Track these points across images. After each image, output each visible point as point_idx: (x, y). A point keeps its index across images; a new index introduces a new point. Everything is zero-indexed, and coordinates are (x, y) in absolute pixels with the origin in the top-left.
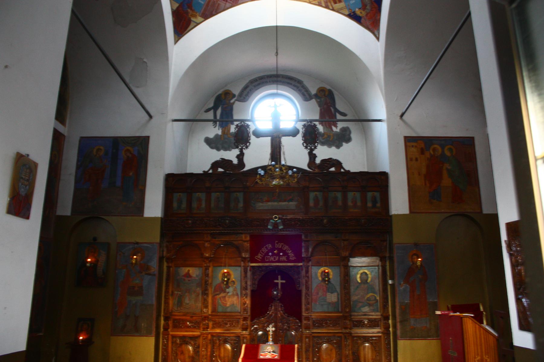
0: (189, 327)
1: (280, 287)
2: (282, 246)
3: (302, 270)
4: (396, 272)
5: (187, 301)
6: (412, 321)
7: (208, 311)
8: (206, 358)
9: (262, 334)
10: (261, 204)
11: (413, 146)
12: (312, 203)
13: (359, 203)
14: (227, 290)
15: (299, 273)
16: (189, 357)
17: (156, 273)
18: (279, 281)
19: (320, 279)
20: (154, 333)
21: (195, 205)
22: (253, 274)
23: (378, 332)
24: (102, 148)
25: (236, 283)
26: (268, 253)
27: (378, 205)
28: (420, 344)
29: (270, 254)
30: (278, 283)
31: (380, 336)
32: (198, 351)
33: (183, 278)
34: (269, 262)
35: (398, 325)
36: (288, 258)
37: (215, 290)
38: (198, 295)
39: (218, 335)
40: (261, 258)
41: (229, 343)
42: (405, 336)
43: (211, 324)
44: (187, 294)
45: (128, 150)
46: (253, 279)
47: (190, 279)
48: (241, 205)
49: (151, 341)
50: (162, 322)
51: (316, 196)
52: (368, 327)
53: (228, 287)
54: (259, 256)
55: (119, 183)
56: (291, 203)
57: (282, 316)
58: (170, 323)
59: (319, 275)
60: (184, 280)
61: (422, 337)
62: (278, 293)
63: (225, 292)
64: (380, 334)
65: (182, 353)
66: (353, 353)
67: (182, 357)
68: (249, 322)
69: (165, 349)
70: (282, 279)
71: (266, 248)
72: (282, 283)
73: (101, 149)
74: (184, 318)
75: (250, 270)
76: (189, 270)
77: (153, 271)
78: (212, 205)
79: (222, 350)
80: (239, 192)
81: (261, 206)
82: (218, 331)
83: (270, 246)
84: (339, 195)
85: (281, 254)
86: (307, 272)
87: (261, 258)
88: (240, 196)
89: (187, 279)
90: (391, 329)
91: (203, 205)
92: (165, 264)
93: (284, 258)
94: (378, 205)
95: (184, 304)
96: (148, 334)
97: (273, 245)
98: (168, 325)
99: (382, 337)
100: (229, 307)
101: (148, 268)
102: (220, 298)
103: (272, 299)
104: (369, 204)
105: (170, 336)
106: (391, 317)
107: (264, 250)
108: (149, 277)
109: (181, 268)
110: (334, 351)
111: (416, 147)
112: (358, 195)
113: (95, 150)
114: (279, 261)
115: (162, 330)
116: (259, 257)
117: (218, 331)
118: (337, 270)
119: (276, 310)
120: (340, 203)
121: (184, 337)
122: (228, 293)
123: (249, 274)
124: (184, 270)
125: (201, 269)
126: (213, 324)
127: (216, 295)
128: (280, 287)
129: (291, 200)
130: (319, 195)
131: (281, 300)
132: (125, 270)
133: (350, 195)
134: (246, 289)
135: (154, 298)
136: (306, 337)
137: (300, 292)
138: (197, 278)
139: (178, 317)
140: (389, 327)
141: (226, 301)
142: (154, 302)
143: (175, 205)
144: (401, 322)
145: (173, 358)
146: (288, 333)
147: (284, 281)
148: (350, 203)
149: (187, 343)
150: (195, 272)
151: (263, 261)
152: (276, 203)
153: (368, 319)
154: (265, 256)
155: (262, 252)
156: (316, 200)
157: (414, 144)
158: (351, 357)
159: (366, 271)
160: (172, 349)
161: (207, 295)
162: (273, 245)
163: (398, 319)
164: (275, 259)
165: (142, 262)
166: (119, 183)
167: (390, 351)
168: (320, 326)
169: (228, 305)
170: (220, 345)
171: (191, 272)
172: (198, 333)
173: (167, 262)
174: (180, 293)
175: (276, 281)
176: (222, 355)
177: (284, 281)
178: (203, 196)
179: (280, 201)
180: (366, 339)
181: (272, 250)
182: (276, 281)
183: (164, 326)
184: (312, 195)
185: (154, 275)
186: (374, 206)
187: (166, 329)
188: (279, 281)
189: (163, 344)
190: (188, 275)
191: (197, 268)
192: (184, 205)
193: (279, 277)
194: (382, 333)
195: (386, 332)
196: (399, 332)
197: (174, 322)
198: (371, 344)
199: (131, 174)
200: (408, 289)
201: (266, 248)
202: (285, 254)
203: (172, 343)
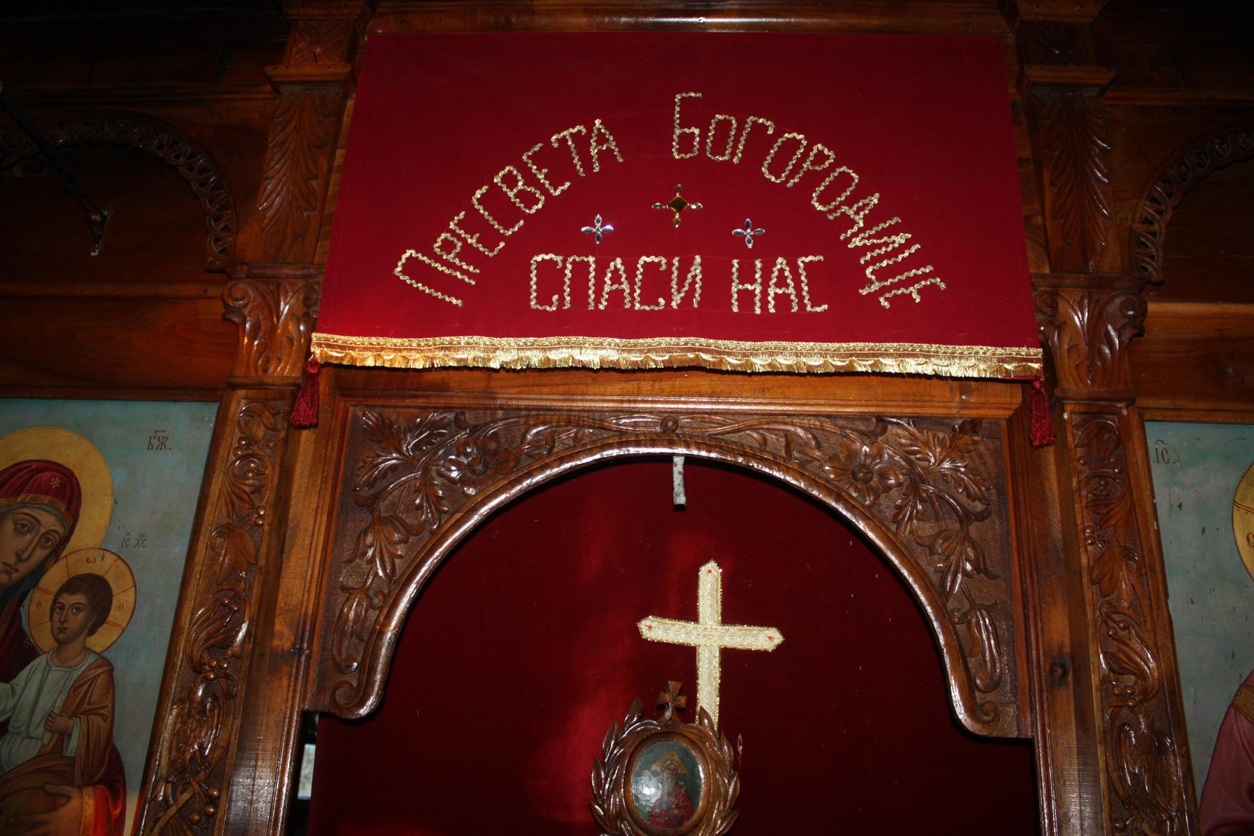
1: (708, 697)
25: (123, 598)
30: (686, 656)
54: (453, 251)
62: (684, 787)
70: (732, 614)
83: (595, 140)
87: (466, 273)
93: (780, 282)
107: (526, 185)
114: (712, 317)
128: (708, 697)
147: (765, 639)
154: (521, 249)
155: (494, 199)
164: (656, 283)
175: (656, 629)
177: (765, 639)
182: (656, 629)
188: (709, 634)
193: (710, 579)
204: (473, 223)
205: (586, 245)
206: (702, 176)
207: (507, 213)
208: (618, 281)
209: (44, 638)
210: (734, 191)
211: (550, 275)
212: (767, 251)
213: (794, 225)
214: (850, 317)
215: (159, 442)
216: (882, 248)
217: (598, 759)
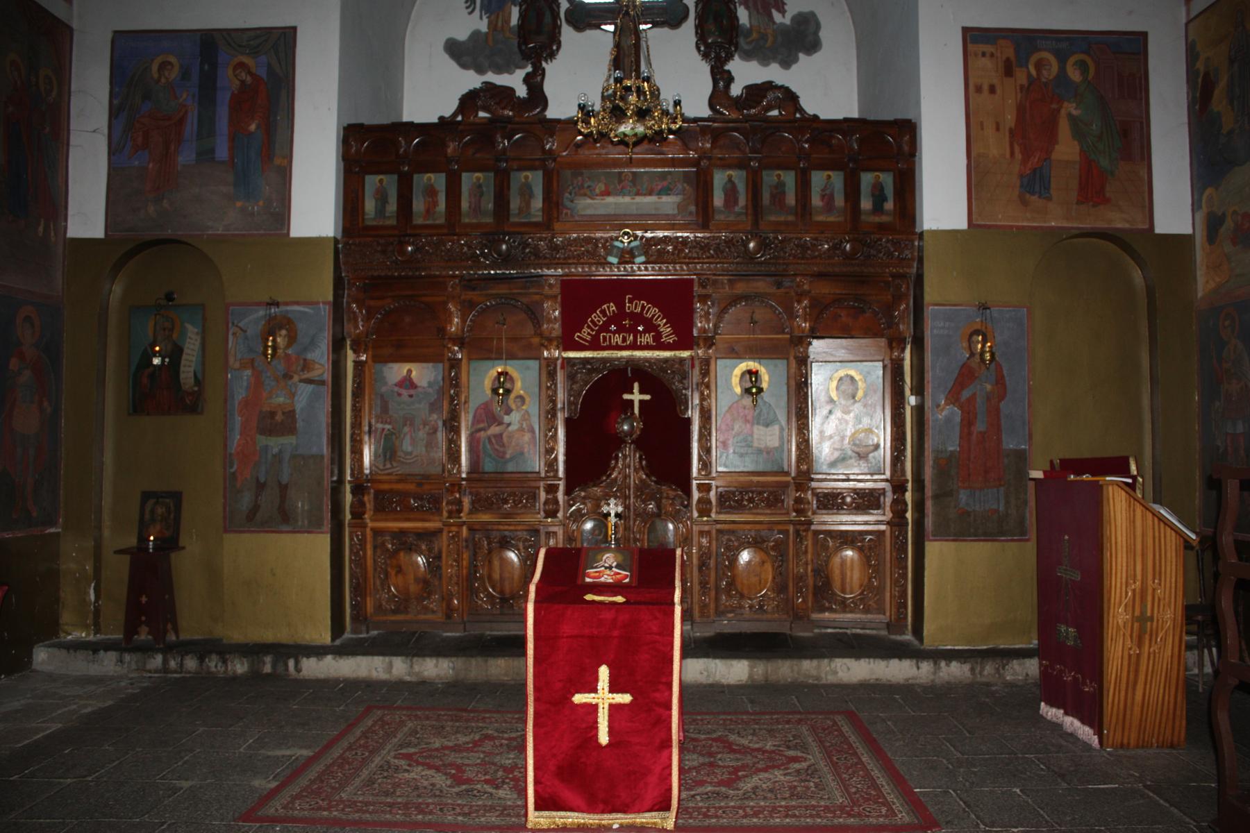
0: (412, 509)
1: (636, 411)
2: (643, 307)
3: (693, 366)
4: (929, 376)
5: (407, 446)
6: (963, 496)
7: (459, 472)
8: (457, 584)
9: (593, 529)
10: (589, 201)
11: (984, 54)
12: (718, 200)
13: (839, 201)
14: (507, 419)
15: (684, 376)
16: (417, 580)
17: (328, 377)
18: (636, 397)
19: (738, 390)
20: (327, 526)
21: (418, 205)
22: (571, 378)
23: (878, 523)
24: (172, 59)
25: (527, 400)
26: (605, 328)
27: (889, 205)
28: (978, 552)
29: (613, 327)
30: (632, 402)
31: (880, 534)
32: (439, 567)
33: (396, 389)
34: (610, 348)
35: (929, 505)
36: (658, 337)
37: (476, 420)
38: (435, 431)
39: (485, 528)
40: (589, 338)
41: (513, 546)
42: (943, 533)
43: (466, 502)
44: (406, 429)
45: (241, 65)
46: (570, 392)
47: (412, 392)
48: (538, 203)
49: (322, 542)
50: (349, 498)
51: (730, 177)
52: (855, 508)
53: (509, 411)
54: (585, 334)
55: (222, 152)
56: (665, 199)
57: (641, 480)
58: (368, 499)
59: (735, 380)
60: (400, 395)
61: (985, 534)
63: (500, 423)
64: (883, 527)
65: (400, 570)
66: (817, 572)
67: (400, 579)
68: (560, 496)
69: (359, 562)
70: (641, 392)
71: (603, 312)
72: (641, 402)
73: (170, 63)
74: (400, 486)
75: (562, 367)
76: (410, 371)
77: (320, 372)
78: (465, 205)
79: (496, 563)
80: (532, 168)
81: (588, 206)
82: (485, 518)
84: (789, 178)
85: (640, 328)
86: (705, 373)
87: (589, 338)
88: (535, 179)
89: (405, 393)
90: (909, 515)
91: (442, 206)
92: (350, 356)
93: (647, 339)
94: (889, 205)
95: (400, 453)
96: (313, 526)
97: (620, 306)
98: (363, 504)
99: (888, 534)
100: (511, 459)
101: (307, 366)
102: (489, 439)
103: (618, 442)
104: (866, 204)
105: (368, 530)
106: (909, 485)
107: (597, 318)
108: (310, 387)
109: (391, 365)
110: (768, 567)
111: (992, 55)
112: (837, 179)
113: (155, 67)
115: (348, 516)
116: (585, 336)
117: (485, 518)
118: (781, 365)
119: (628, 465)
120: (791, 200)
121: (403, 532)
122: (509, 425)
123: (560, 376)
124: (396, 371)
125: (440, 365)
126: (473, 503)
127: (480, 430)
128: (636, 411)
129: (666, 191)
130: (739, 176)
131: (640, 444)
132: (248, 372)
133: (818, 179)
134: (553, 413)
135: (325, 440)
136: (701, 533)
137: (688, 422)
138: (430, 390)
139: (386, 487)
140: (906, 511)
141: (503, 446)
142: (325, 450)
143: (370, 206)
144: (936, 497)
145: (378, 582)
146: (659, 523)
147: (647, 397)
148: (816, 201)
149: (412, 549)
150: (423, 374)
151: (595, 345)
152: (627, 199)
153: (855, 491)
156: (731, 193)
157: (988, 48)
158: (810, 581)
159: (852, 373)
160: (375, 561)
161: (457, 431)
162: (620, 306)
163: (929, 492)
164: (624, 340)
165: (290, 351)
166: (222, 152)
167: (906, 568)
168: (739, 507)
169: (508, 456)
170: (490, 551)
171: (414, 374)
172: (437, 525)
173: (355, 351)
174: (388, 427)
175: (626, 397)
176: (496, 576)
177: (647, 397)
178: (439, 180)
179: (638, 194)
180: (848, 539)
181: (616, 319)
182: (626, 397)
183: (352, 506)
184: (719, 179)
185: (322, 383)
186: (878, 208)
187: (358, 514)
188: (636, 397)
189: (351, 550)
190: (407, 383)
191: (430, 365)
192: (392, 207)
193: (636, 385)
194: (888, 523)
195: (898, 521)
196: (929, 522)
197: (376, 498)
198: (860, 550)
199: (253, 127)
200: (958, 419)
201: (603, 312)
202: (651, 327)
203: (375, 548)
204: (589, 327)
205: (610, 331)
206: (632, 316)
207: (595, 325)
208: (618, 339)
209: (513, 407)
210: (638, 318)
211: (605, 338)
212: (645, 331)
213: (651, 327)
214: (661, 346)
215: (528, 368)
216: (666, 330)
217: (617, 422)
